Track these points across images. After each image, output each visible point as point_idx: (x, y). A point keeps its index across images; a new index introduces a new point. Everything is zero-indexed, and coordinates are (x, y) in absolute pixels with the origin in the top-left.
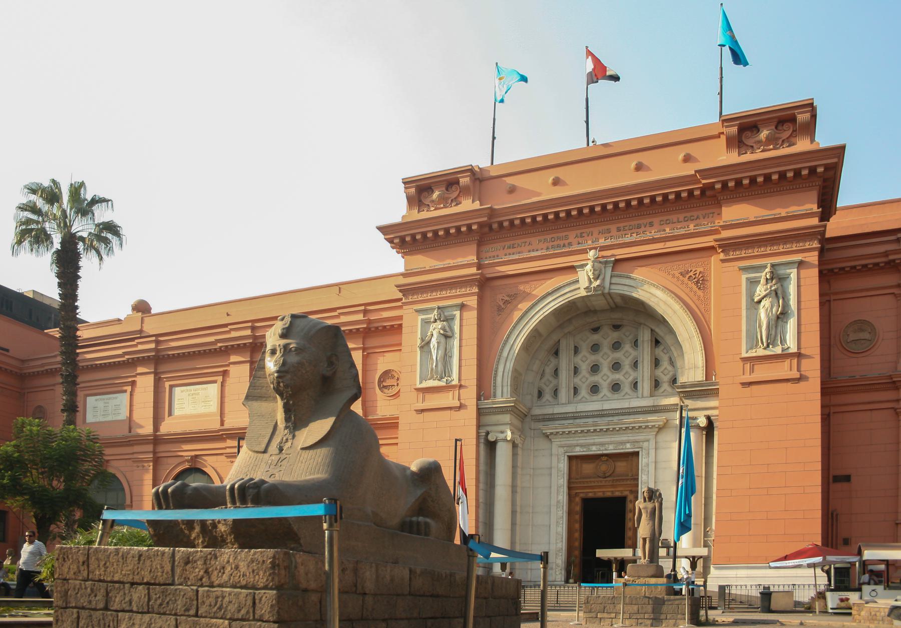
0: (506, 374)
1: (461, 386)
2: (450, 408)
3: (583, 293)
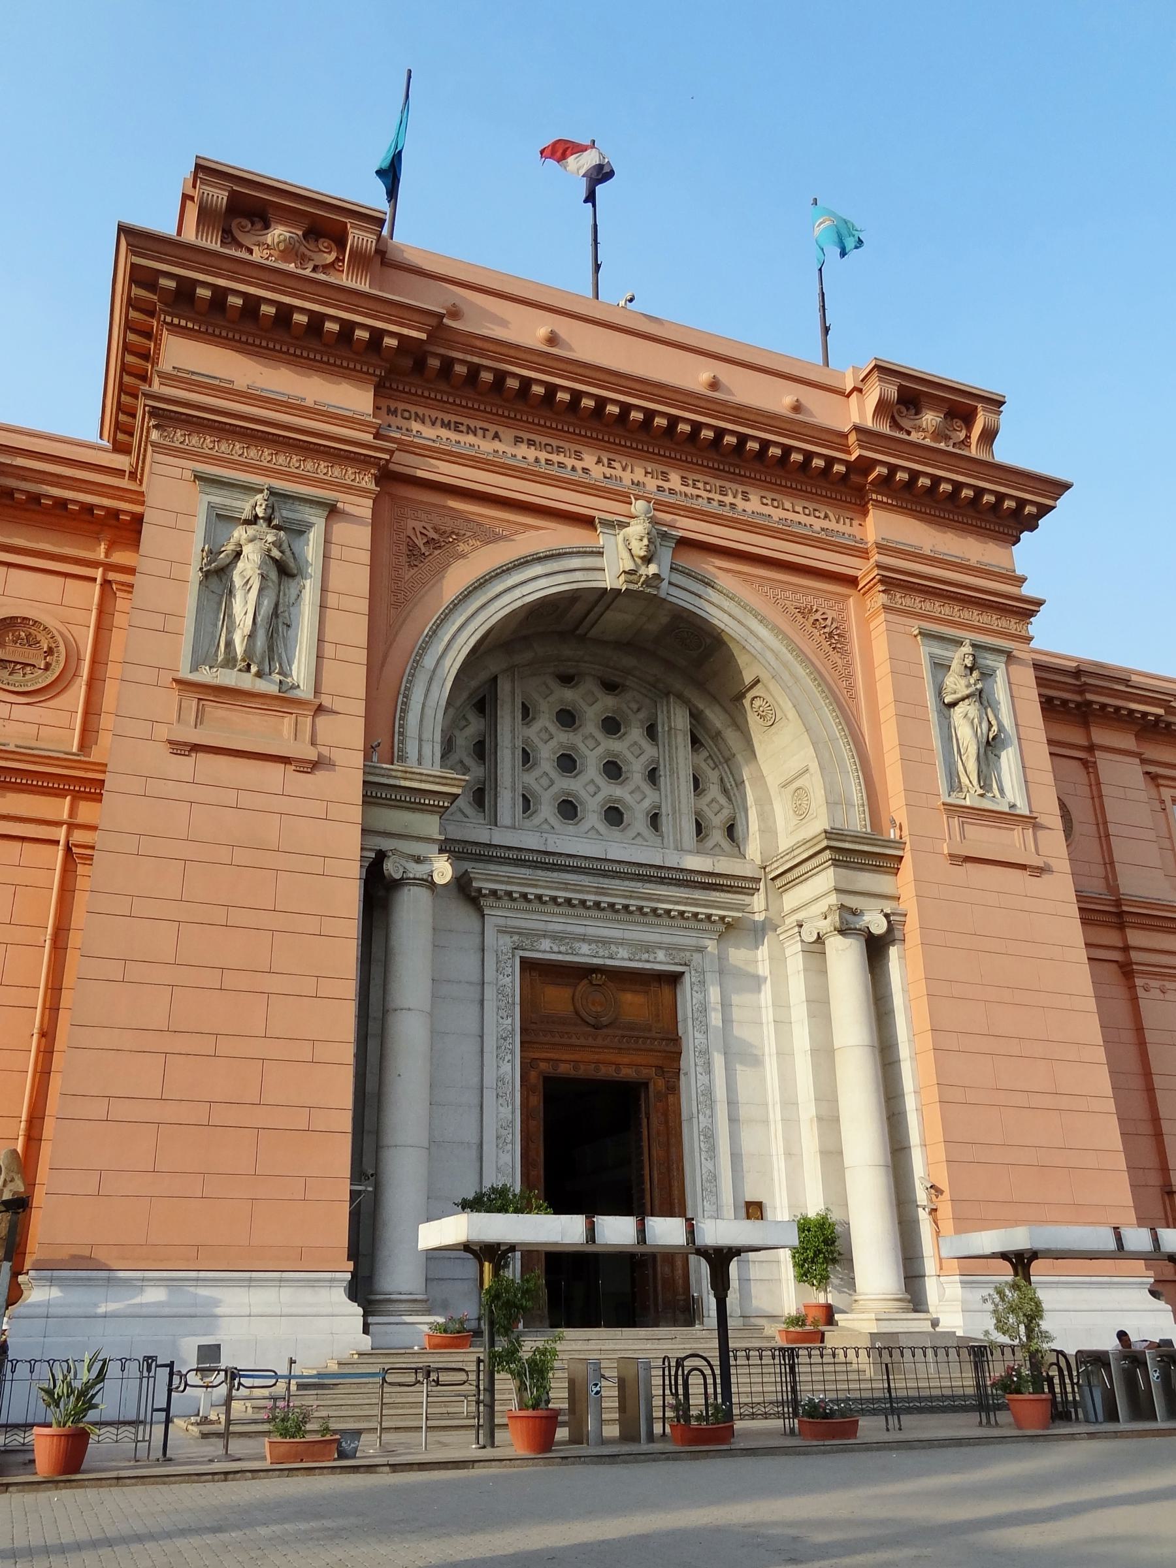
0: (429, 712)
1: (320, 709)
2: (285, 760)
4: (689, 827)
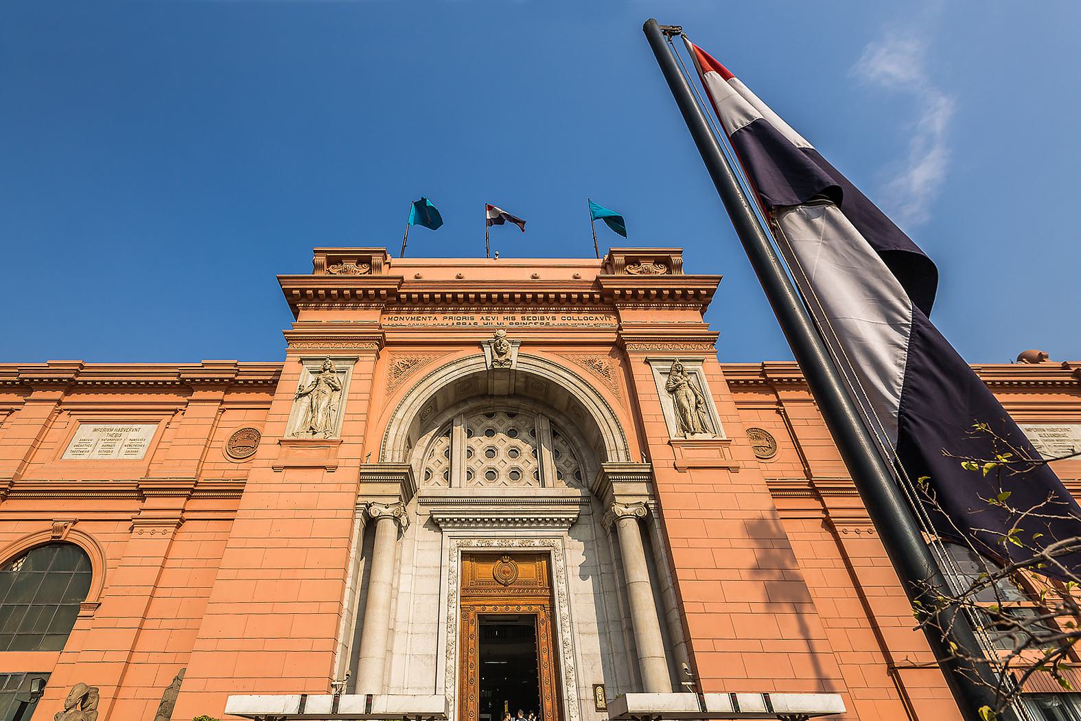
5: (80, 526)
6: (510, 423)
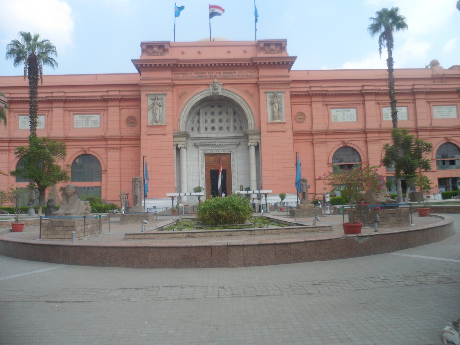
3: (212, 95)
4: (232, 129)
5: (91, 149)
6: (219, 110)
